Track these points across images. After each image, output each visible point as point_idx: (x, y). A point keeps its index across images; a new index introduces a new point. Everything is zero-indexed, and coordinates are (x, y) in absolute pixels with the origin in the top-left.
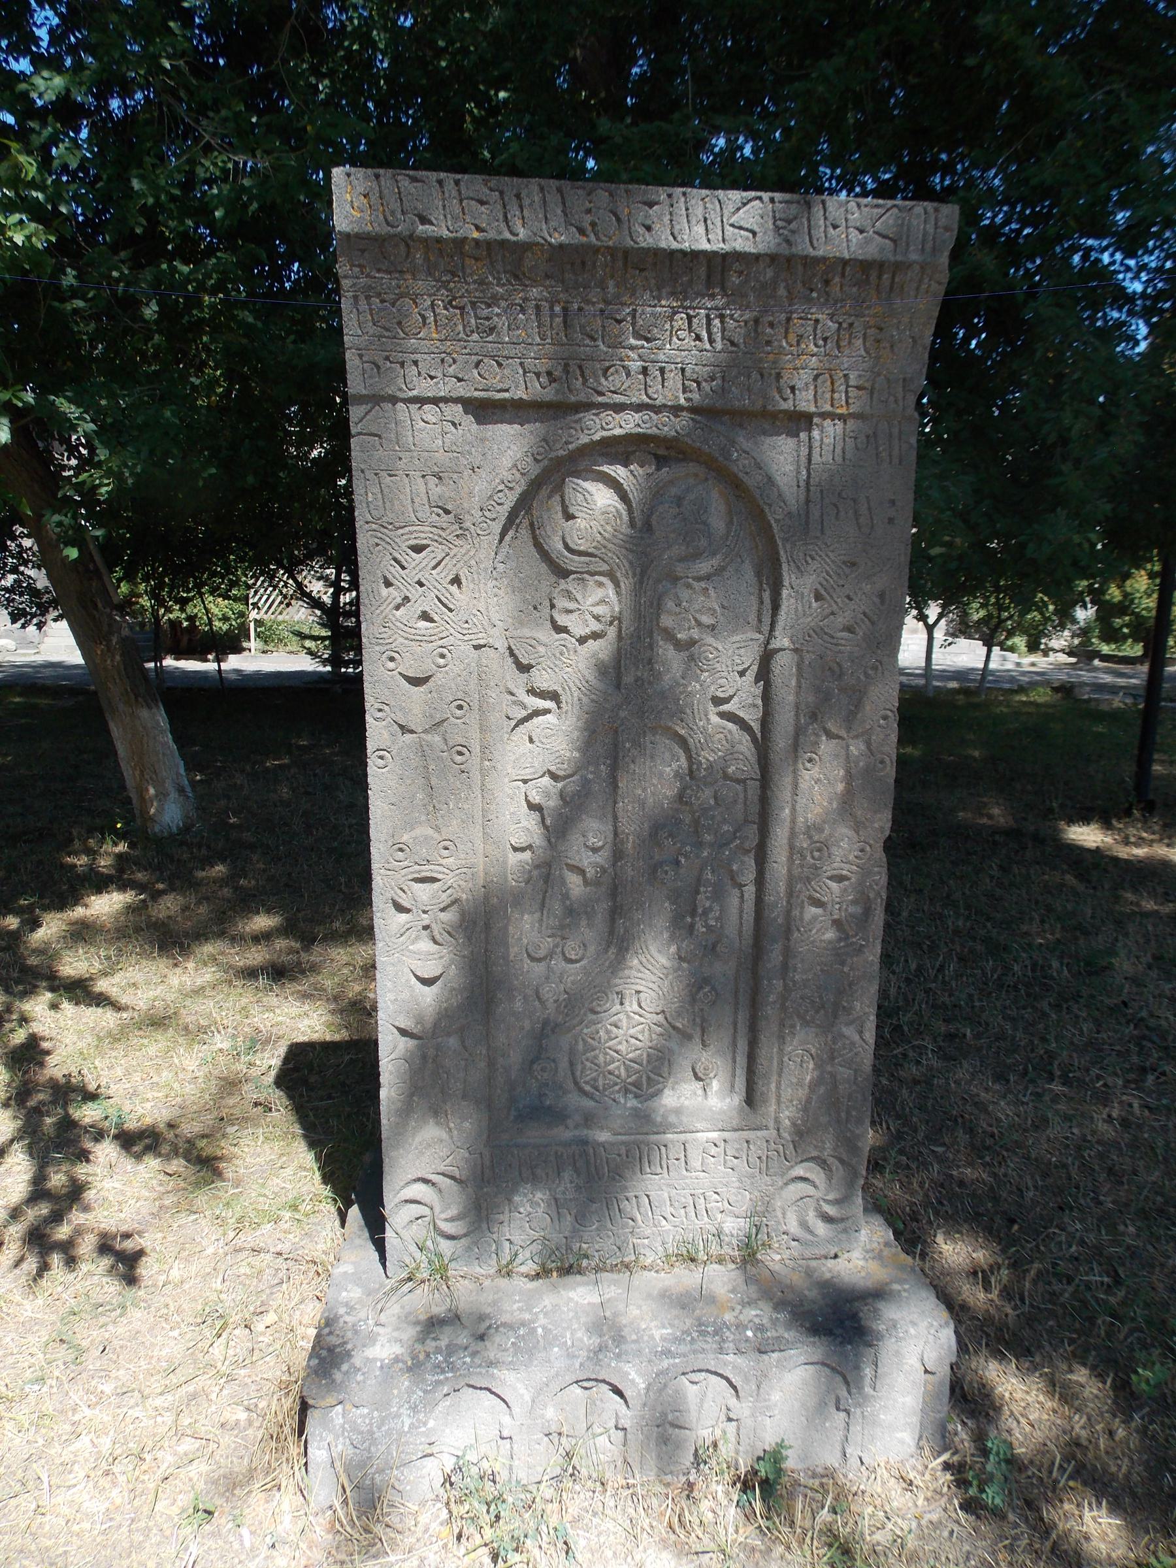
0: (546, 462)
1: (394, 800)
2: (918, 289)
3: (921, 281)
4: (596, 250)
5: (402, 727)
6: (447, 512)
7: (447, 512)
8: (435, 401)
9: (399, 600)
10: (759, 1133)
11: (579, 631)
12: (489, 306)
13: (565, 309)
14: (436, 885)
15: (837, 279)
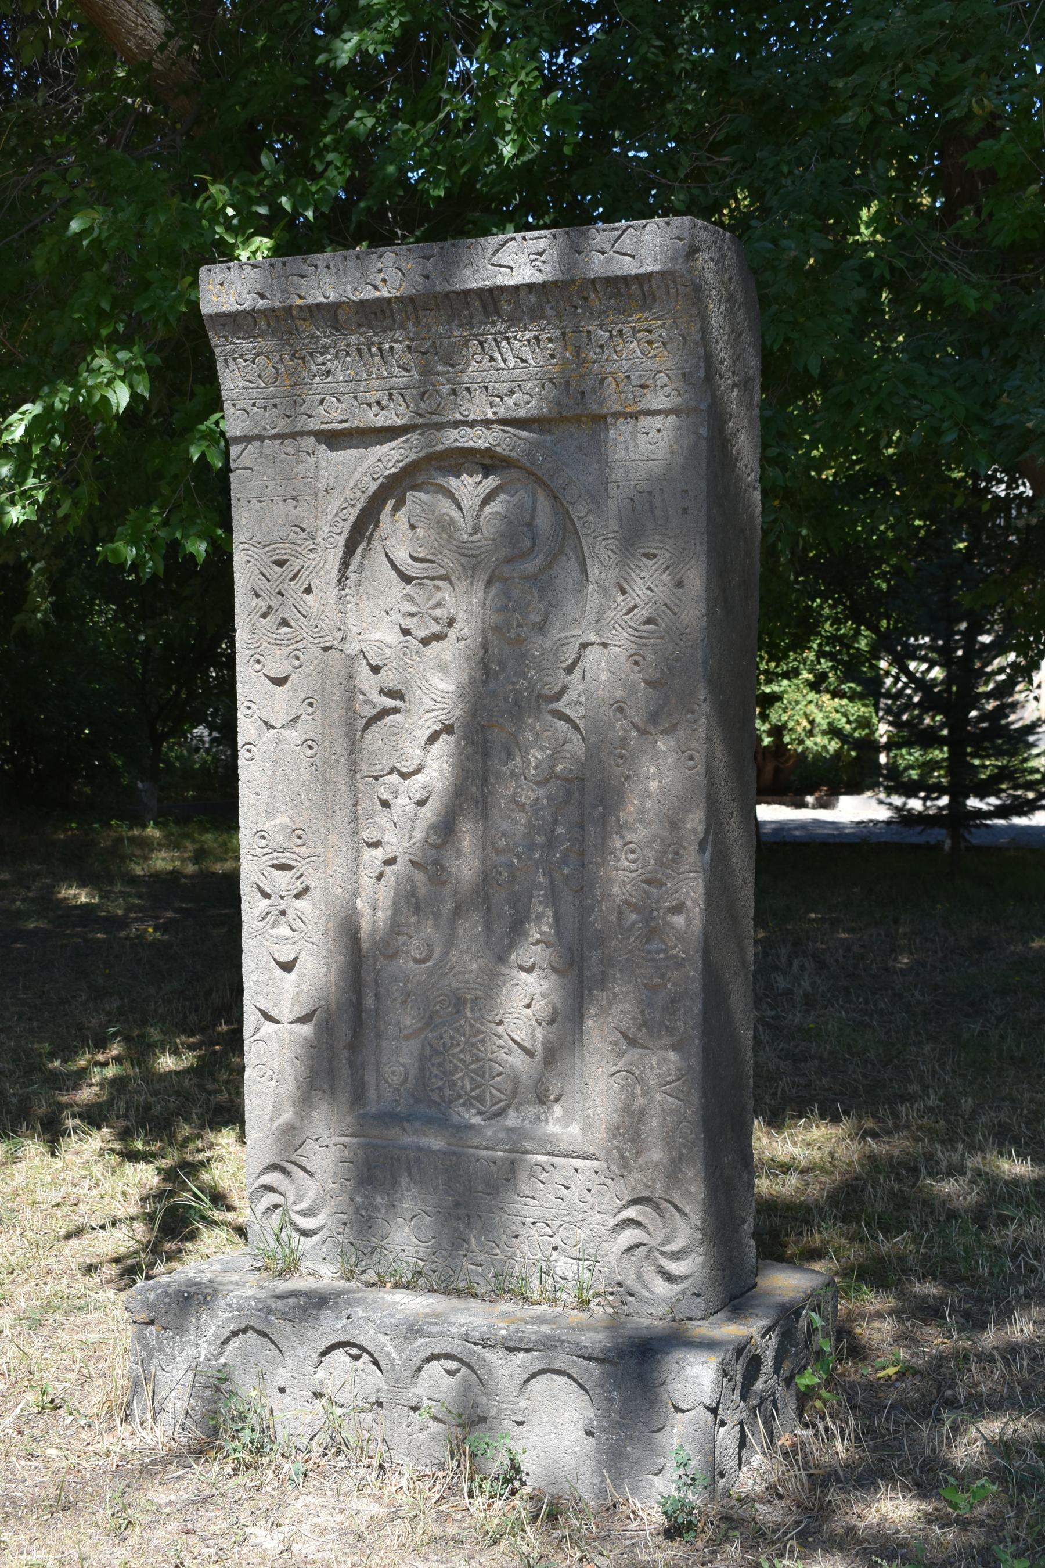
0: (381, 480)
1: (257, 790)
5: (266, 723)
6: (303, 530)
7: (303, 530)
8: (293, 435)
9: (264, 609)
10: (588, 1163)
12: (322, 354)
13: (380, 349)
15: (592, 296)
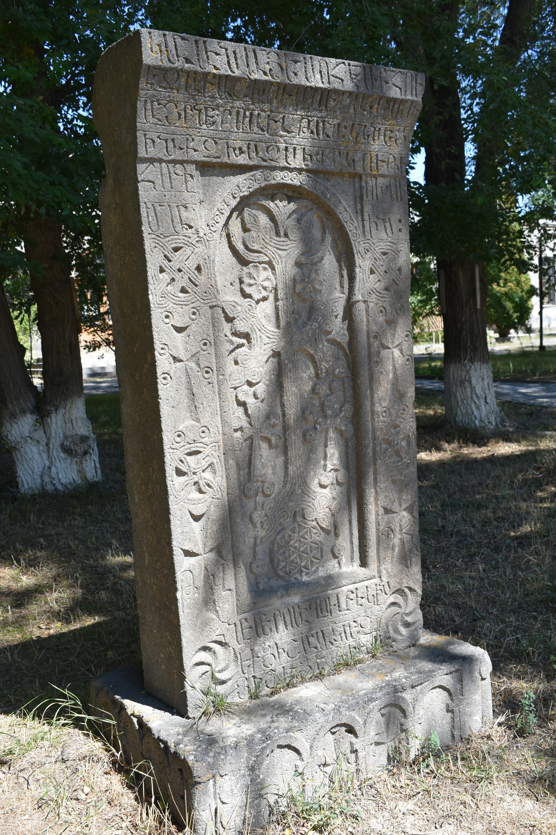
1: (173, 405)
2: (408, 112)
3: (410, 109)
4: (271, 83)
5: (174, 358)
7: (191, 227)
8: (182, 162)
11: (257, 296)
12: (213, 110)
13: (251, 114)
14: (199, 456)
